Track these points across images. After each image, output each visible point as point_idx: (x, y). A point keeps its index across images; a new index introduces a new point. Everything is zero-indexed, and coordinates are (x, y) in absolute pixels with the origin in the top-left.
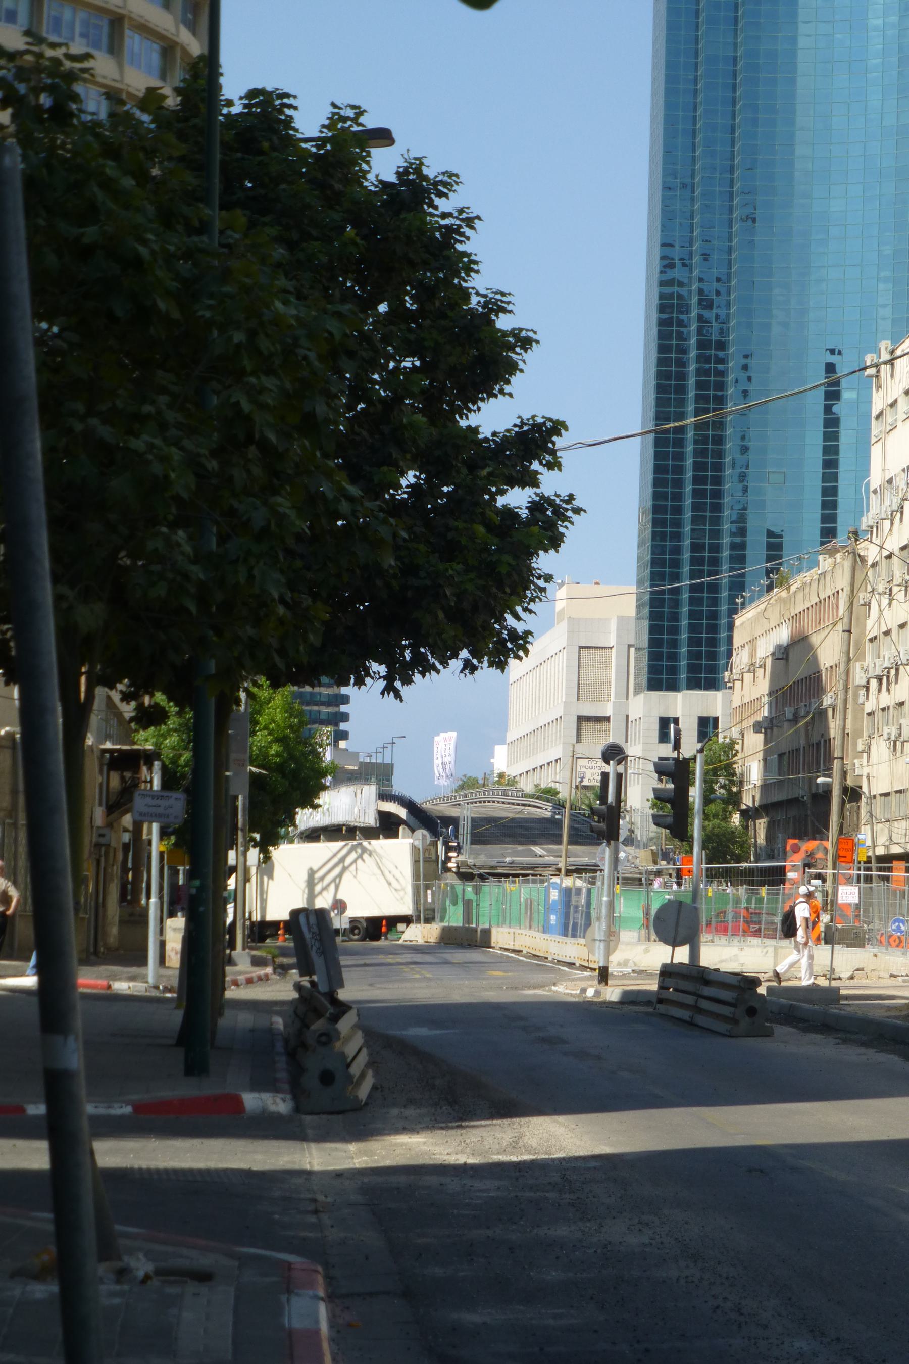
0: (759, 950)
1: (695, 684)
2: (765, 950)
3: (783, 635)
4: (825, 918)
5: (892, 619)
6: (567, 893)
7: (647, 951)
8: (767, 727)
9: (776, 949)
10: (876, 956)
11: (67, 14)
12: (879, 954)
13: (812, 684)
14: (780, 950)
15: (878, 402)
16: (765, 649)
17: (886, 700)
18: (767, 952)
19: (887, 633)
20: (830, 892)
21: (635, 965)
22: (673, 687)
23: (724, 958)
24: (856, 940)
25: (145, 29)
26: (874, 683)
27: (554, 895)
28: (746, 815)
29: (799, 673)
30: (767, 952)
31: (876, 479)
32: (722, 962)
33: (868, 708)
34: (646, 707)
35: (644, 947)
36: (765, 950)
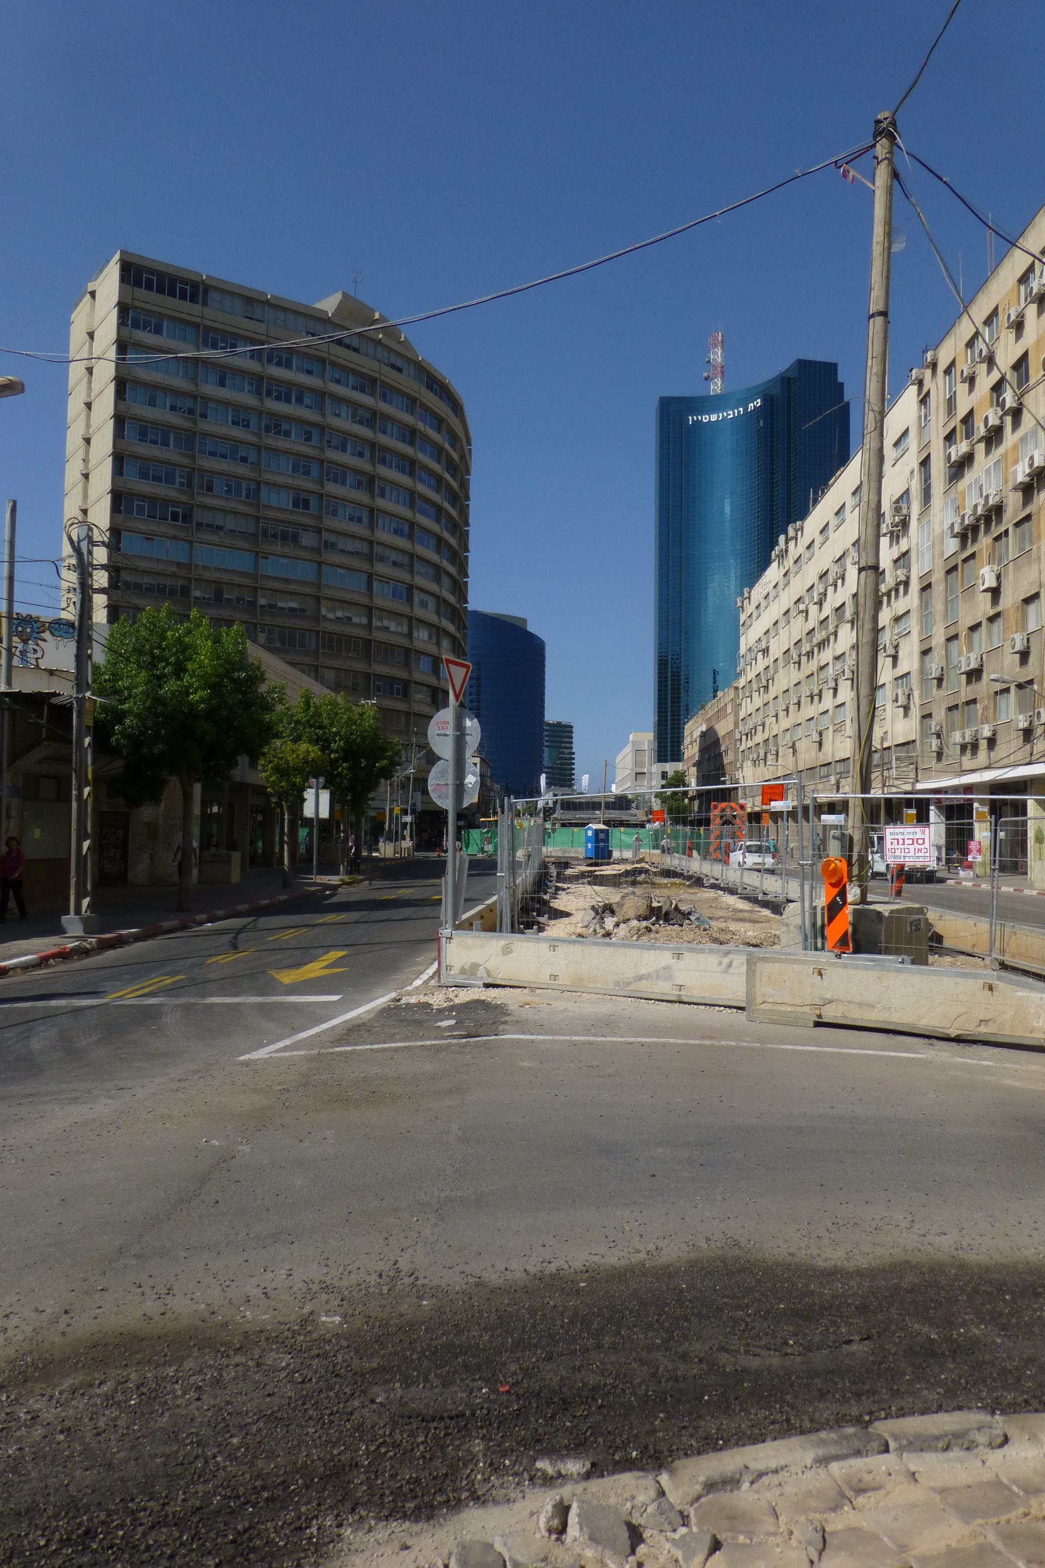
0: (713, 960)
1: (673, 760)
2: (726, 961)
3: (704, 728)
4: (853, 893)
5: (751, 709)
6: (597, 832)
7: (507, 951)
8: (698, 764)
9: (750, 963)
10: (991, 988)
11: (388, 457)
12: (1000, 985)
13: (717, 743)
14: (760, 966)
15: (743, 617)
16: (697, 734)
17: (750, 744)
18: (730, 965)
19: (750, 715)
20: (856, 838)
21: (488, 972)
22: (666, 762)
23: (644, 971)
24: (922, 944)
25: (425, 468)
26: (744, 737)
27: (590, 833)
28: (692, 799)
29: (709, 741)
30: (730, 965)
31: (743, 650)
32: (640, 978)
33: (741, 749)
34: (657, 768)
35: (502, 943)
36: (726, 961)
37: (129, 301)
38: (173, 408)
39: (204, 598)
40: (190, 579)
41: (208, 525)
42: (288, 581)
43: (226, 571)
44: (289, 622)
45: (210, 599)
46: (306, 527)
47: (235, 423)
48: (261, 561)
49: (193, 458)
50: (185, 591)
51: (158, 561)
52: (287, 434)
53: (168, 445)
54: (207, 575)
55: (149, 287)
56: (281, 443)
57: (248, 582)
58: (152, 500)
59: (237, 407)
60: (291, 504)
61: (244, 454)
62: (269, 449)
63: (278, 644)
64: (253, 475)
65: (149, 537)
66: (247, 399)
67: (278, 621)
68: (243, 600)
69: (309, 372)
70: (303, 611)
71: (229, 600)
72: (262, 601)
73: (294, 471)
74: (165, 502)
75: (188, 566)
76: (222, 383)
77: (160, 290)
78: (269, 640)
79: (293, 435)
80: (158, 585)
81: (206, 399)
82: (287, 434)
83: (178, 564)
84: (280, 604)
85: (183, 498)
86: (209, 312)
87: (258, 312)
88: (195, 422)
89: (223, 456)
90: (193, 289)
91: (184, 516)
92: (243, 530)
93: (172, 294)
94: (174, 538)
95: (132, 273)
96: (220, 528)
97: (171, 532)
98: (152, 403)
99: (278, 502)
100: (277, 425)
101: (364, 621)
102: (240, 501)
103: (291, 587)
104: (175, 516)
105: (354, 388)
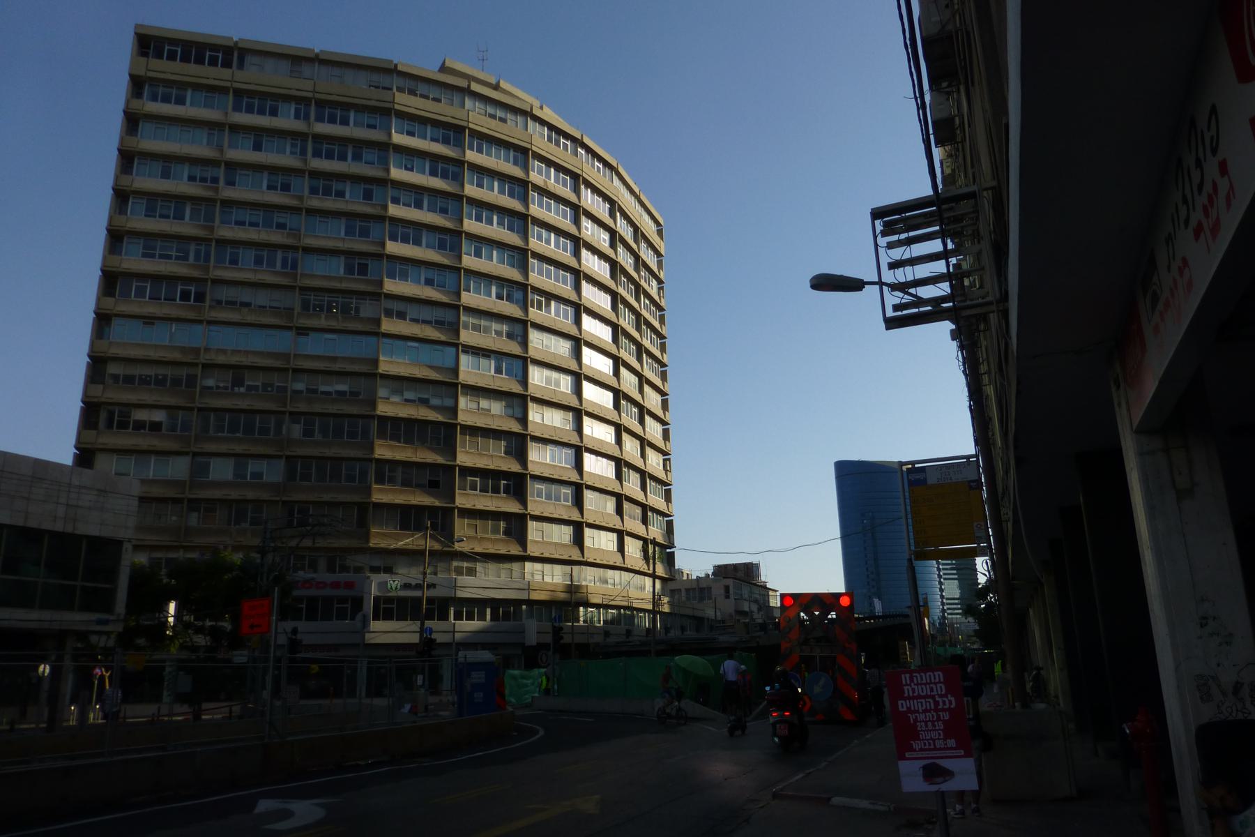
37: (142, 72)
38: (192, 178)
39: (218, 387)
40: (196, 365)
41: (228, 303)
42: (334, 359)
43: (247, 353)
44: (333, 409)
45: (226, 388)
46: (361, 295)
47: (270, 187)
48: (302, 339)
49: (211, 229)
50: (191, 381)
51: (156, 347)
52: (340, 194)
53: (183, 218)
54: (221, 359)
55: (172, 57)
56: (330, 204)
57: (278, 364)
58: (156, 278)
59: (273, 170)
60: (342, 271)
61: (281, 220)
62: (311, 212)
63: (318, 436)
64: (290, 241)
65: (149, 320)
66: (286, 159)
67: (317, 408)
68: (272, 385)
69: (374, 127)
70: (352, 393)
71: (256, 388)
72: (300, 386)
73: (346, 234)
74: (172, 279)
75: (196, 351)
76: (257, 147)
77: (185, 59)
78: (308, 433)
79: (347, 195)
80: (156, 376)
81: (232, 166)
82: (340, 194)
83: (183, 350)
84: (323, 388)
85: (196, 273)
86: (239, 75)
87: (306, 69)
88: (216, 190)
89: (256, 225)
90: (229, 54)
91: (195, 292)
92: (275, 304)
93: (200, 61)
94: (178, 320)
95: (147, 43)
96: (248, 305)
97: (174, 312)
98: (166, 175)
99: (329, 272)
100: (325, 182)
101: (449, 402)
102: (276, 273)
103: (336, 367)
104: (185, 296)
105: (433, 140)
